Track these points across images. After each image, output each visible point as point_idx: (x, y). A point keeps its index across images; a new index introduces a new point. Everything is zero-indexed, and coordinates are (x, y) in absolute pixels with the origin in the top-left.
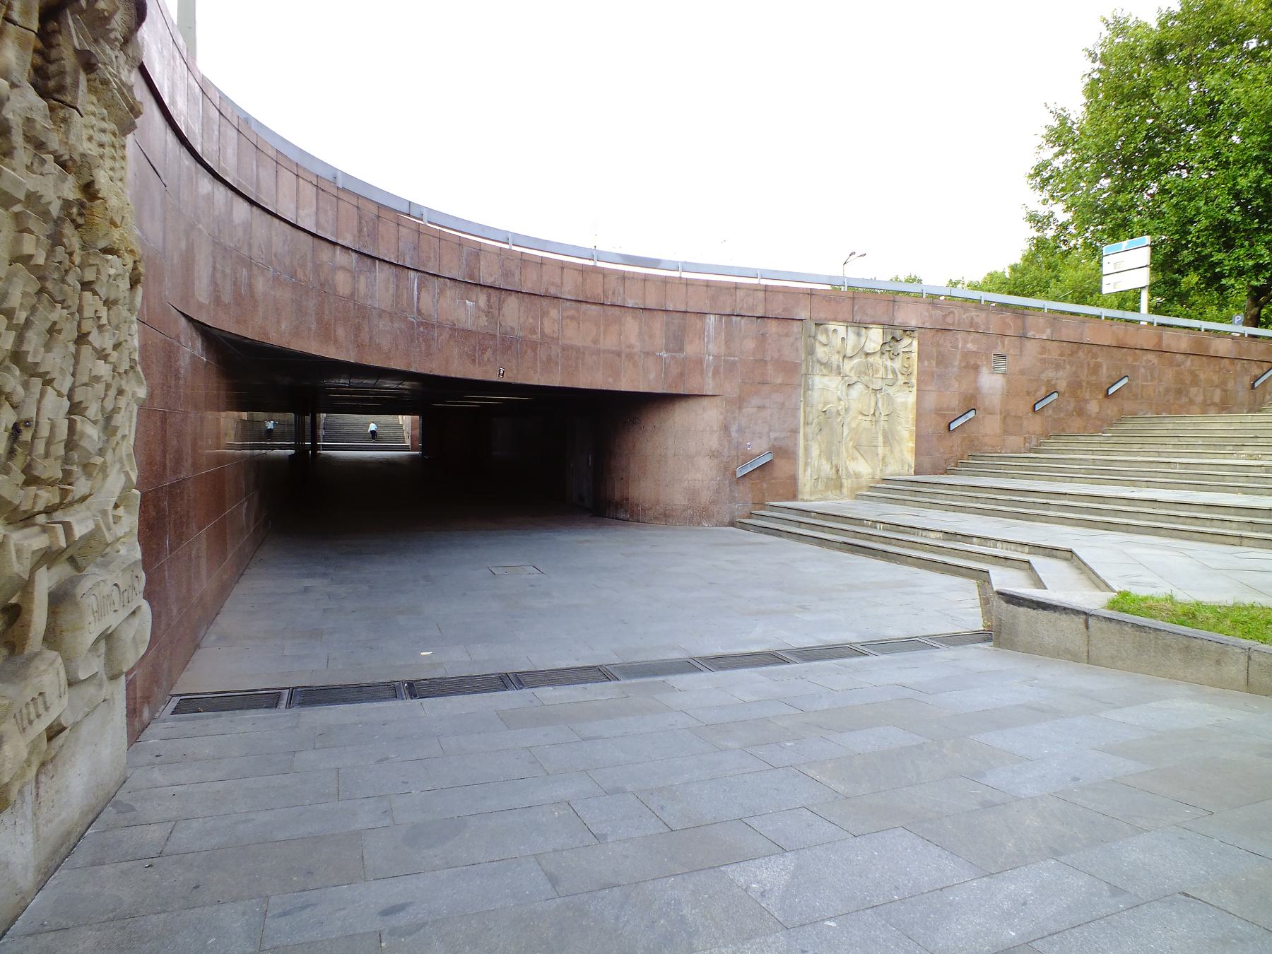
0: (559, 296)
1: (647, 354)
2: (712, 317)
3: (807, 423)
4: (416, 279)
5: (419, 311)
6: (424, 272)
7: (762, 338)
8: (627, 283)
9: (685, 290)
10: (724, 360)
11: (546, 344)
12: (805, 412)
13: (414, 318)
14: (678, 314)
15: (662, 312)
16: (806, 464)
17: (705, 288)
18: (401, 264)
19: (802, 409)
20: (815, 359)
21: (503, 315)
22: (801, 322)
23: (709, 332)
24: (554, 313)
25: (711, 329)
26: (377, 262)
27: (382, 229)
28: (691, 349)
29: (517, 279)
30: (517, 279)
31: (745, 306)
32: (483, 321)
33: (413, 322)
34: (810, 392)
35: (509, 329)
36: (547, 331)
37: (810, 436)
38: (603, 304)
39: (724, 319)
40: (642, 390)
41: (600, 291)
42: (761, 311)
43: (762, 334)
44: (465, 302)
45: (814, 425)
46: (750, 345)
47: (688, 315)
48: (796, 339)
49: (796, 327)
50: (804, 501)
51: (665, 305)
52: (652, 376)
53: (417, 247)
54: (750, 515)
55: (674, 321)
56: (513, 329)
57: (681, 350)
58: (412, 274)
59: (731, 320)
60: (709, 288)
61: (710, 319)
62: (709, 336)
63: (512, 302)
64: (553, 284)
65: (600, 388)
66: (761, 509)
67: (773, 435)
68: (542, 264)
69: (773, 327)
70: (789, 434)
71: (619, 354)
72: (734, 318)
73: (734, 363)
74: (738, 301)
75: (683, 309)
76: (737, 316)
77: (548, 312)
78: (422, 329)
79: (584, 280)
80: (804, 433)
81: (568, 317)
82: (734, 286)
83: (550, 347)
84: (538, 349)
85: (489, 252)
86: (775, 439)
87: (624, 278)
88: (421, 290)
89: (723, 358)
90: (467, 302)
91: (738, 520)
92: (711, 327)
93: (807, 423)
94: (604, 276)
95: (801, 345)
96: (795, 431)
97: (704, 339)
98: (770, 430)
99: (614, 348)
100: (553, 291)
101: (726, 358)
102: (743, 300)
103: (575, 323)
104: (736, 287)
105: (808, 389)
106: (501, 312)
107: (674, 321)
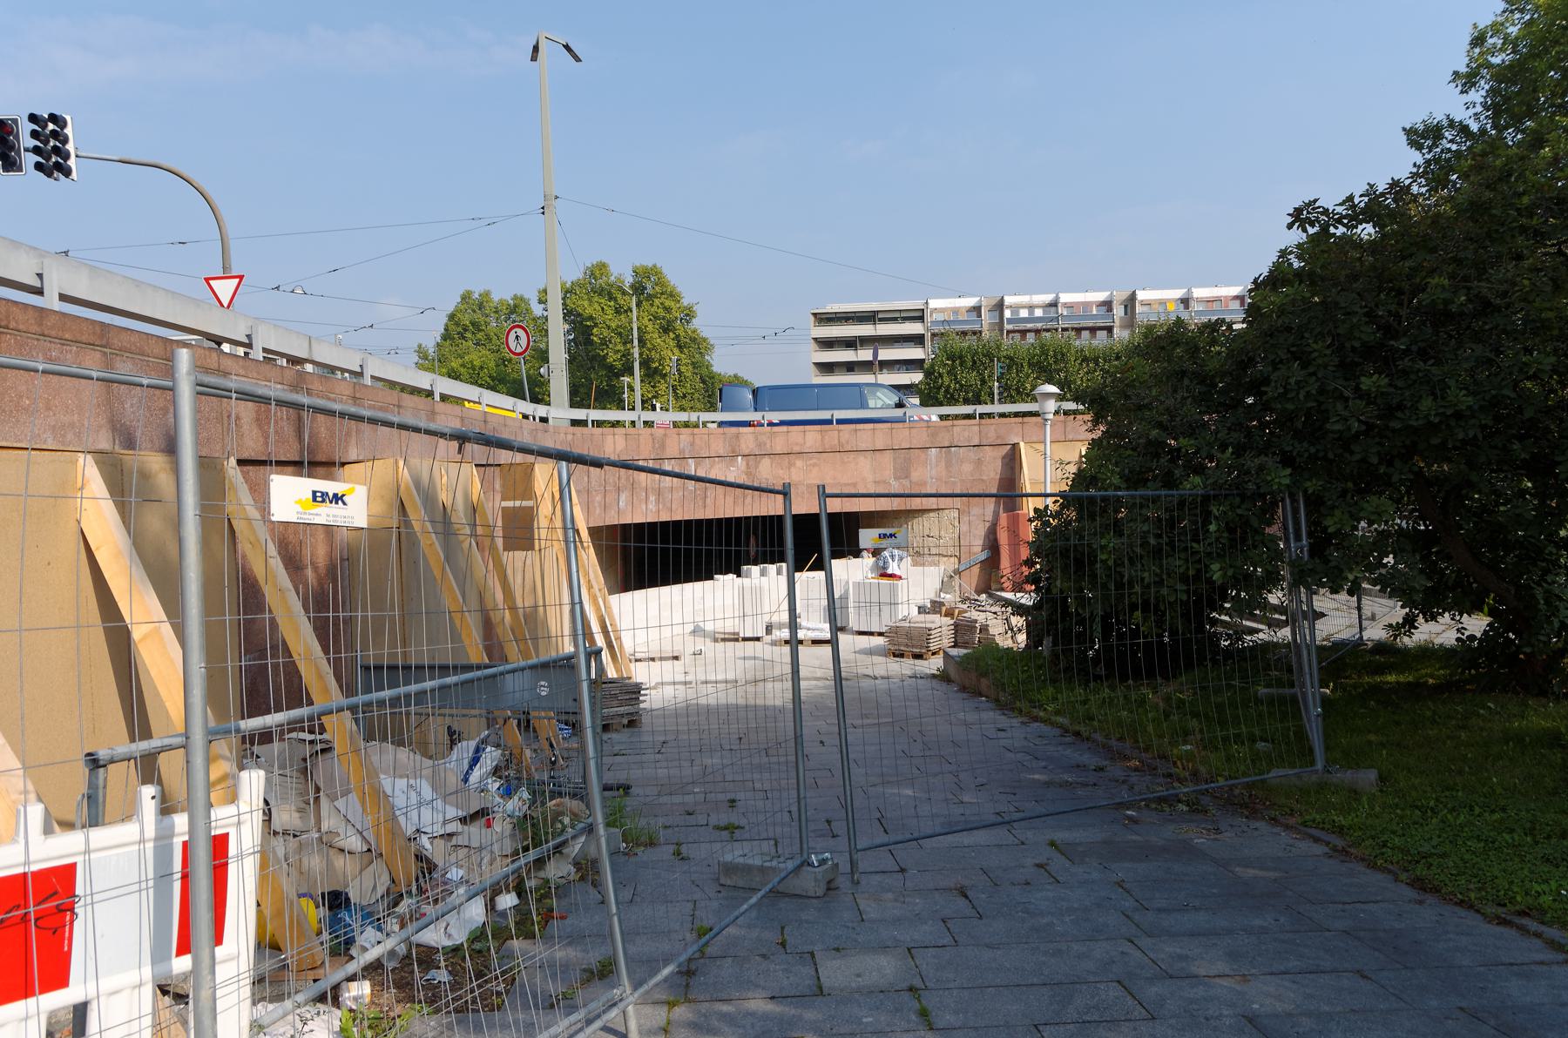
7: (979, 462)
8: (859, 433)
23: (931, 460)
24: (799, 463)
27: (668, 441)
30: (768, 446)
32: (744, 476)
41: (836, 442)
46: (967, 468)
53: (692, 444)
59: (950, 452)
63: (766, 461)
64: (797, 444)
72: (953, 449)
77: (795, 464)
79: (823, 437)
100: (796, 449)
103: (816, 469)
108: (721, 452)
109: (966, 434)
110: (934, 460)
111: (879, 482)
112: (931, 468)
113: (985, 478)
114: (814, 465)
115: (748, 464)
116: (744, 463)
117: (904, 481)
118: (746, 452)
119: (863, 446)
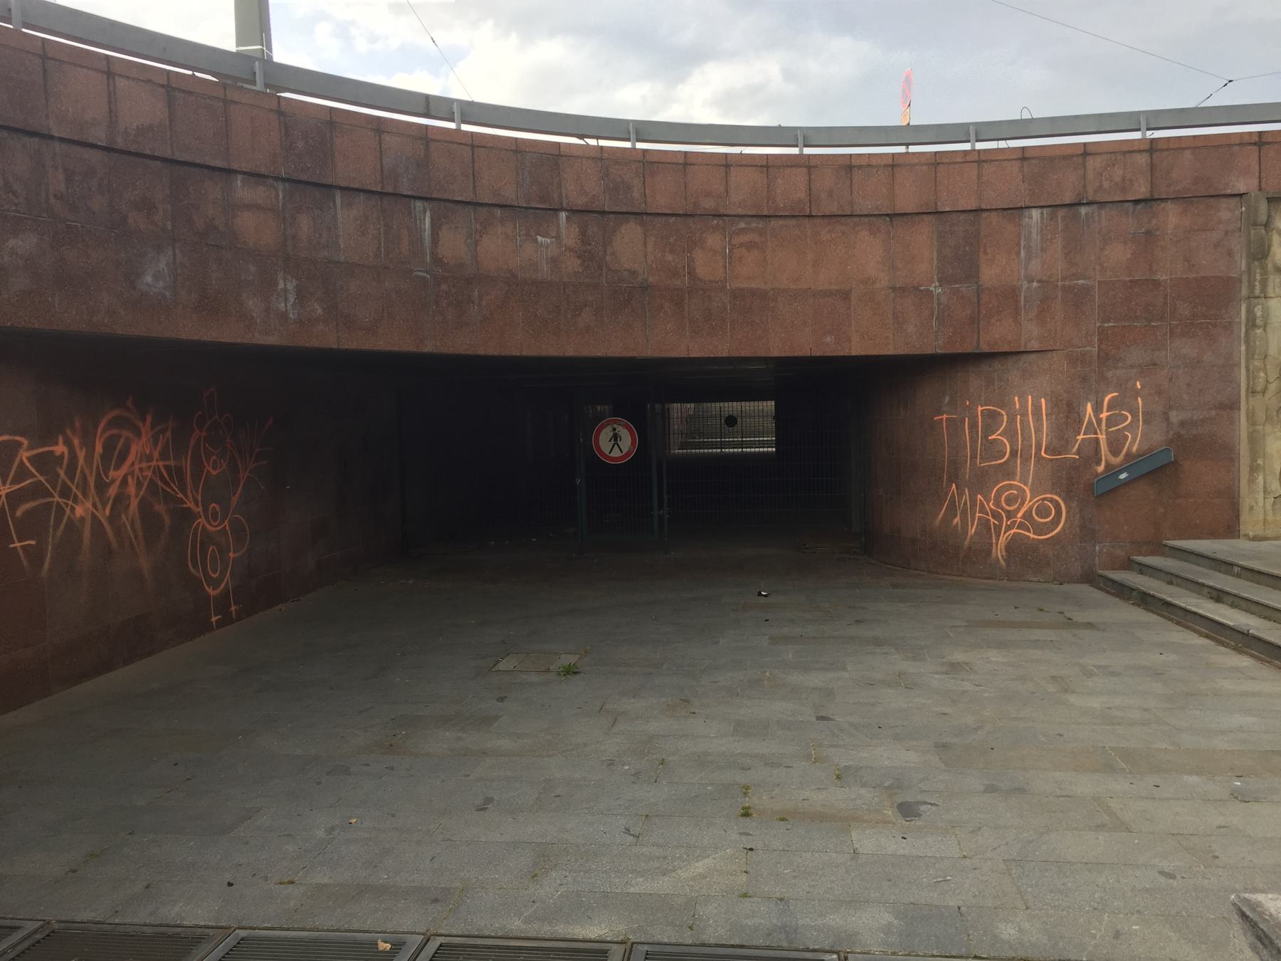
0: (722, 211)
1: (899, 291)
2: (1035, 213)
3: (1252, 392)
4: (428, 214)
5: (437, 260)
6: (445, 201)
8: (857, 175)
9: (975, 172)
10: (1063, 286)
11: (701, 292)
12: (1248, 370)
13: (427, 272)
14: (962, 217)
15: (930, 217)
16: (1254, 469)
17: (1018, 164)
18: (390, 190)
19: (1243, 365)
20: (1270, 266)
21: (613, 254)
22: (1238, 199)
24: (713, 240)
25: (1034, 235)
26: (338, 196)
28: (990, 274)
29: (636, 194)
30: (636, 194)
31: (1106, 184)
32: (572, 264)
33: (425, 278)
34: (1259, 331)
35: (626, 273)
36: (702, 271)
37: (1261, 416)
38: (810, 216)
39: (1061, 213)
40: (890, 350)
42: (1143, 189)
43: (1148, 233)
44: (536, 240)
45: (1269, 394)
46: (1119, 254)
47: (985, 215)
48: (1226, 233)
49: (1226, 212)
50: (1255, 539)
51: (936, 204)
52: (911, 329)
54: (1129, 565)
55: (955, 228)
56: (633, 273)
57: (972, 274)
58: (419, 204)
60: (1025, 163)
61: (1031, 218)
62: (1028, 248)
65: (809, 354)
66: (1153, 553)
67: (1175, 417)
68: (686, 164)
69: (1172, 218)
70: (1213, 413)
71: (845, 295)
73: (1086, 290)
74: (1090, 175)
75: (973, 205)
76: (1089, 203)
78: (444, 287)
80: (1248, 409)
81: (741, 245)
82: (1082, 151)
83: (709, 297)
84: (686, 301)
85: (578, 157)
86: (1182, 424)
87: (728, 166)
88: (440, 228)
89: (1060, 283)
90: (539, 238)
91: (1100, 572)
92: (1034, 231)
93: (1252, 392)
94: (809, 168)
95: (1237, 245)
96: (1233, 406)
97: (1018, 253)
98: (1171, 408)
99: (834, 287)
100: (708, 204)
101: (1067, 283)
102: (1101, 174)
104: (1086, 151)
105: (1254, 326)
106: (609, 250)
107: (955, 228)
108: (510, 194)
109: (1118, 173)
110: (1035, 236)
111: (903, 289)
112: (1029, 258)
113: (1162, 277)
114: (750, 246)
115: (583, 233)
116: (575, 230)
117: (964, 288)
118: (580, 202)
119: (866, 206)
